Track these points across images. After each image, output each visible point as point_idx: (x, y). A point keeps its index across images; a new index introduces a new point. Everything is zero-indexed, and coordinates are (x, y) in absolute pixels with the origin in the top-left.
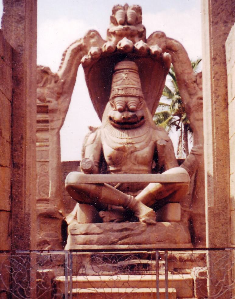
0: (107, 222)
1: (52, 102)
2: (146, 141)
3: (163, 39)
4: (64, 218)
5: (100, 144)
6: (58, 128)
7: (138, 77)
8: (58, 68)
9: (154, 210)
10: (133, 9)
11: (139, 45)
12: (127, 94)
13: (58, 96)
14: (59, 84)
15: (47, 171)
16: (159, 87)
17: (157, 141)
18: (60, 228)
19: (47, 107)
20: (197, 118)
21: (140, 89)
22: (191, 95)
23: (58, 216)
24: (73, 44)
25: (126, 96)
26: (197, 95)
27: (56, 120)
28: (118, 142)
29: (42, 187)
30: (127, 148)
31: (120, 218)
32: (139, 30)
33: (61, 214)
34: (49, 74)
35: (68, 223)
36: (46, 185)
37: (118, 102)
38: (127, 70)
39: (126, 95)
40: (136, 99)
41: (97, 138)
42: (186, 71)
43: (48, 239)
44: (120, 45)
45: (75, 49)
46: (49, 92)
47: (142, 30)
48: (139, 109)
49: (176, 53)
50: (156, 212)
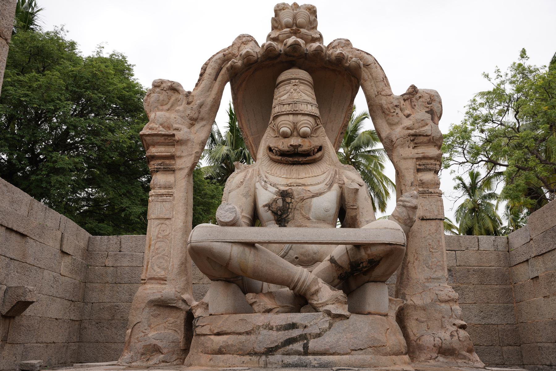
0: (259, 312)
1: (181, 129)
2: (325, 183)
4: (189, 308)
5: (252, 190)
6: (188, 167)
7: (314, 93)
8: (194, 87)
9: (344, 292)
10: (304, 9)
11: (315, 45)
12: (297, 110)
13: (191, 122)
14: (195, 105)
15: (167, 233)
16: (343, 115)
17: (344, 184)
18: (183, 324)
19: (173, 135)
20: (404, 155)
22: (391, 124)
23: (180, 305)
24: (217, 53)
25: (295, 114)
27: (185, 156)
28: (282, 184)
29: (158, 258)
31: (283, 307)
32: (313, 36)
33: (184, 301)
35: (195, 317)
36: (164, 255)
37: (282, 123)
38: (297, 81)
39: (294, 112)
40: (311, 119)
41: (247, 179)
42: (383, 93)
43: (160, 344)
44: (285, 45)
45: (219, 58)
46: (177, 117)
47: (319, 36)
48: (314, 136)
49: (367, 68)
50: (347, 296)
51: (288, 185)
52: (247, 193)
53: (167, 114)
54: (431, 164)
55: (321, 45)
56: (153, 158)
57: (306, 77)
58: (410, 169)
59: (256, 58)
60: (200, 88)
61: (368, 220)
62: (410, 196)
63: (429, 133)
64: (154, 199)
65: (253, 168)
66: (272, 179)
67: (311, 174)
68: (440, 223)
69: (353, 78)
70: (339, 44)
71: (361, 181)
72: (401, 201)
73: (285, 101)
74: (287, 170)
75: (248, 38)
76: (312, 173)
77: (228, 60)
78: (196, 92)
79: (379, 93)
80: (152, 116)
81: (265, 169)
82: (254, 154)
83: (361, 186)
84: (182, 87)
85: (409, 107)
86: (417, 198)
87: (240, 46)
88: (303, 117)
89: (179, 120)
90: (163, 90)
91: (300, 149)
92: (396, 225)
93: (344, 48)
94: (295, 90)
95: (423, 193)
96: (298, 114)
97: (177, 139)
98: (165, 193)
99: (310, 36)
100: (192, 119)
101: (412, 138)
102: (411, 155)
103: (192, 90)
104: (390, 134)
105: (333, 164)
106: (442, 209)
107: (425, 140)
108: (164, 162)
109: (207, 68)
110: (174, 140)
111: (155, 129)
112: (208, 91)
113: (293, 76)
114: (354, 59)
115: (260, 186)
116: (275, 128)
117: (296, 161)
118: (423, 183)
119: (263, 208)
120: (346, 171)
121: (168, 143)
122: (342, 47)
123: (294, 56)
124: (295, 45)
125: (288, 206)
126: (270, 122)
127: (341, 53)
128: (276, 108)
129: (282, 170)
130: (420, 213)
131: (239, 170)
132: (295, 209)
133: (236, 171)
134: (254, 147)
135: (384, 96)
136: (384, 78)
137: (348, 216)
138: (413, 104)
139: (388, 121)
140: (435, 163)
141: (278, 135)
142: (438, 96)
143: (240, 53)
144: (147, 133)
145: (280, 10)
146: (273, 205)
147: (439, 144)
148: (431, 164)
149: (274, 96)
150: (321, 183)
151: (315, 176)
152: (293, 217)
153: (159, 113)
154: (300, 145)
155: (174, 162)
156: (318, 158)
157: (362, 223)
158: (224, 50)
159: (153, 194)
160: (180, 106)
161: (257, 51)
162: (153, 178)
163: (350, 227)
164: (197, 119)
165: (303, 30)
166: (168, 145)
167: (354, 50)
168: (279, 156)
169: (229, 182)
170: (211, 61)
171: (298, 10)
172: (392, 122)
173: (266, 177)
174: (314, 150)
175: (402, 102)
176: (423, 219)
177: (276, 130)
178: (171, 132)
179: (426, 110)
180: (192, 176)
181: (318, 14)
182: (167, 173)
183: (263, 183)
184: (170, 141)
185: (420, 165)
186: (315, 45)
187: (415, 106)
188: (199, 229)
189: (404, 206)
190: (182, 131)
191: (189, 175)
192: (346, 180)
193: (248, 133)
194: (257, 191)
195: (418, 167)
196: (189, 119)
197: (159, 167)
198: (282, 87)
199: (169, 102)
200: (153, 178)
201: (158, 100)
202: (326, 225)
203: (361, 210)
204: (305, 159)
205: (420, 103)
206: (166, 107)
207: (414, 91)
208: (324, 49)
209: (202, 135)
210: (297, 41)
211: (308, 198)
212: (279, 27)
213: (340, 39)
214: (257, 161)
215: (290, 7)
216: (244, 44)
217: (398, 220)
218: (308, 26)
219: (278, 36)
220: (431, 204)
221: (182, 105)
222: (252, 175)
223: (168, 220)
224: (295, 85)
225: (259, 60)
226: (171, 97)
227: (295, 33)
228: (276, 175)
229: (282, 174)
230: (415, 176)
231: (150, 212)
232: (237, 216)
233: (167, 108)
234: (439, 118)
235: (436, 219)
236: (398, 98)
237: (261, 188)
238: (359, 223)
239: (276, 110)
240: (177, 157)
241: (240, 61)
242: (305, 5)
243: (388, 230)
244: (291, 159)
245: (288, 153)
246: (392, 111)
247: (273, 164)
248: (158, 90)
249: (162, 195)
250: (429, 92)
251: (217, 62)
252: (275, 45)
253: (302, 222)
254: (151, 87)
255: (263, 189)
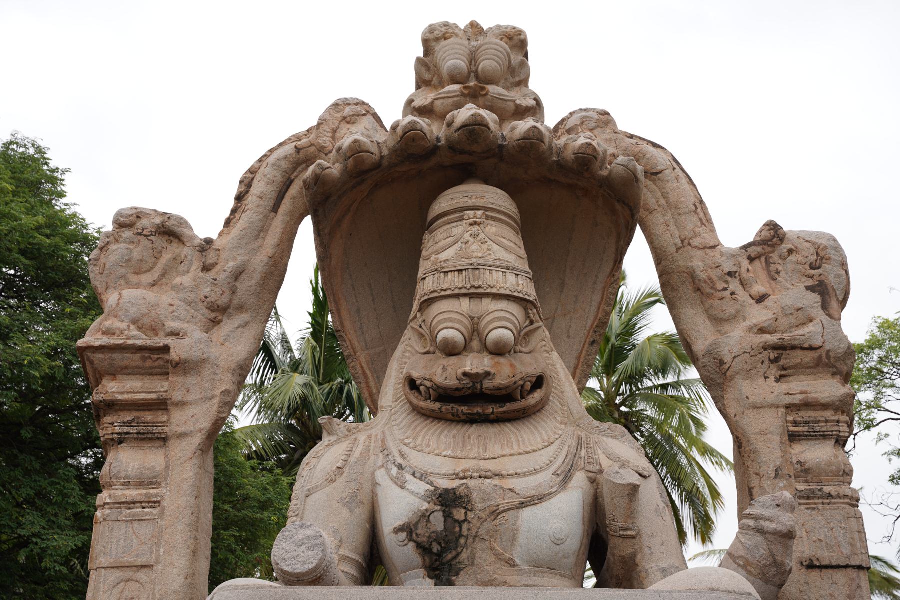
1: (186, 334)
3: (608, 134)
5: (367, 487)
6: (201, 431)
7: (522, 244)
8: (220, 227)
11: (524, 125)
12: (480, 287)
13: (213, 315)
16: (597, 298)
17: (601, 472)
19: (166, 349)
20: (753, 399)
21: (528, 273)
22: (717, 321)
24: (281, 145)
26: (745, 319)
27: (196, 402)
28: (444, 472)
30: (476, 497)
32: (518, 102)
34: (186, 240)
37: (441, 317)
38: (480, 213)
39: (473, 291)
40: (515, 310)
41: (353, 459)
42: (696, 242)
44: (450, 125)
45: (286, 158)
46: (177, 302)
47: (532, 103)
48: (524, 350)
49: (654, 181)
51: (457, 476)
52: (355, 495)
53: (151, 296)
54: (827, 421)
55: (539, 125)
56: (111, 406)
57: (500, 203)
58: (772, 433)
59: (376, 157)
60: (236, 231)
61: (664, 566)
62: (774, 504)
63: (817, 342)
64: (108, 516)
65: (369, 433)
66: (418, 460)
67: (514, 446)
68: (859, 577)
69: (618, 207)
70: (582, 123)
71: (644, 464)
72: (751, 517)
73: (451, 263)
74: (454, 437)
75: (359, 108)
76: (519, 445)
77: (309, 161)
78: (225, 240)
79: (685, 243)
80: (111, 299)
81: (399, 435)
82: (371, 395)
83: (644, 477)
84: (189, 227)
85: (763, 275)
86: (792, 509)
87: (338, 128)
88: (494, 302)
89: (182, 310)
90: (140, 234)
91: (487, 384)
92: (740, 582)
93: (596, 132)
94: (474, 236)
95: (808, 496)
96: (481, 296)
97: (176, 359)
98: (138, 499)
99: (512, 104)
100: (213, 308)
101: (773, 355)
102: (771, 399)
103: (214, 236)
104: (715, 345)
105: (571, 420)
106: (861, 540)
107: (806, 360)
108: (138, 418)
109: (255, 181)
110: (168, 361)
111: (118, 332)
112: (257, 238)
113: (470, 203)
114: (621, 159)
115: (387, 478)
116: (425, 330)
117: (478, 413)
118: (807, 471)
119: (393, 536)
120: (605, 439)
121: (152, 368)
122: (591, 130)
123: (470, 153)
124: (475, 127)
125: (457, 529)
126: (412, 316)
127: (590, 145)
128: (426, 282)
129: (442, 437)
130: (802, 549)
131: (333, 439)
132: (476, 537)
133: (326, 439)
134: (371, 380)
135: (699, 249)
136: (699, 205)
137: (614, 556)
138: (773, 268)
139: (711, 312)
140: (836, 418)
141: (432, 349)
142: (838, 249)
143: (338, 145)
144: (97, 344)
145: (437, 40)
146: (420, 526)
147: (845, 369)
148: (827, 421)
149: (421, 252)
150: (542, 469)
151: (528, 453)
152: (472, 558)
153: (129, 294)
154: (487, 374)
155: (165, 418)
156: (534, 406)
157: (652, 576)
158: (298, 138)
159: (108, 501)
160: (184, 275)
161: (380, 141)
162: (109, 459)
163: (619, 585)
164: (228, 307)
165: (491, 88)
166: (152, 374)
167: (620, 136)
168: (437, 400)
169: (308, 468)
170: (265, 165)
171: (481, 40)
172: (722, 315)
173: (403, 456)
174: (522, 386)
175: (745, 263)
176: (811, 566)
177: (428, 336)
178: (160, 341)
179: (807, 284)
180: (211, 454)
181: (530, 49)
182: (147, 445)
183: (395, 471)
184: (156, 364)
185: (796, 424)
186: (524, 125)
187: (778, 273)
188: (226, 593)
189: (760, 531)
190: (187, 340)
191: (203, 450)
192: (605, 463)
193: (357, 344)
194: (380, 491)
195: (792, 429)
196: (207, 308)
197: (126, 430)
198: (442, 229)
199: (155, 264)
200: (109, 459)
201: (129, 261)
202: (556, 581)
203: (646, 540)
204: (501, 410)
205: (790, 267)
206: (147, 278)
207: (774, 237)
208: (547, 134)
209: (239, 348)
210: (480, 115)
211: (509, 510)
212: (435, 81)
213: (585, 110)
214: (380, 414)
215: (461, 34)
216: (348, 123)
217: (744, 567)
218: (506, 79)
219: (433, 103)
220: (832, 525)
221: (188, 272)
222: (367, 449)
223: (146, 570)
224: (475, 223)
225: (385, 163)
226: (161, 252)
227: (475, 95)
228: (428, 450)
229: (443, 447)
230: (785, 452)
231: (97, 548)
232: (328, 559)
233: (151, 281)
234: (843, 303)
235: (846, 567)
236: (733, 255)
237: (390, 483)
238: (643, 574)
239: (427, 286)
240: (173, 404)
241: (337, 165)
242: (499, 27)
243: (721, 595)
244: (465, 409)
245: (458, 394)
246: (720, 286)
247: (420, 421)
248: (127, 234)
249: (131, 504)
250: (812, 239)
251: (279, 167)
252: (424, 125)
253: (495, 573)
254: (109, 227)
255: (394, 486)
